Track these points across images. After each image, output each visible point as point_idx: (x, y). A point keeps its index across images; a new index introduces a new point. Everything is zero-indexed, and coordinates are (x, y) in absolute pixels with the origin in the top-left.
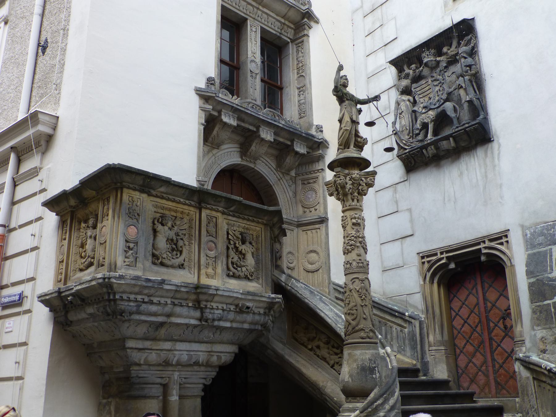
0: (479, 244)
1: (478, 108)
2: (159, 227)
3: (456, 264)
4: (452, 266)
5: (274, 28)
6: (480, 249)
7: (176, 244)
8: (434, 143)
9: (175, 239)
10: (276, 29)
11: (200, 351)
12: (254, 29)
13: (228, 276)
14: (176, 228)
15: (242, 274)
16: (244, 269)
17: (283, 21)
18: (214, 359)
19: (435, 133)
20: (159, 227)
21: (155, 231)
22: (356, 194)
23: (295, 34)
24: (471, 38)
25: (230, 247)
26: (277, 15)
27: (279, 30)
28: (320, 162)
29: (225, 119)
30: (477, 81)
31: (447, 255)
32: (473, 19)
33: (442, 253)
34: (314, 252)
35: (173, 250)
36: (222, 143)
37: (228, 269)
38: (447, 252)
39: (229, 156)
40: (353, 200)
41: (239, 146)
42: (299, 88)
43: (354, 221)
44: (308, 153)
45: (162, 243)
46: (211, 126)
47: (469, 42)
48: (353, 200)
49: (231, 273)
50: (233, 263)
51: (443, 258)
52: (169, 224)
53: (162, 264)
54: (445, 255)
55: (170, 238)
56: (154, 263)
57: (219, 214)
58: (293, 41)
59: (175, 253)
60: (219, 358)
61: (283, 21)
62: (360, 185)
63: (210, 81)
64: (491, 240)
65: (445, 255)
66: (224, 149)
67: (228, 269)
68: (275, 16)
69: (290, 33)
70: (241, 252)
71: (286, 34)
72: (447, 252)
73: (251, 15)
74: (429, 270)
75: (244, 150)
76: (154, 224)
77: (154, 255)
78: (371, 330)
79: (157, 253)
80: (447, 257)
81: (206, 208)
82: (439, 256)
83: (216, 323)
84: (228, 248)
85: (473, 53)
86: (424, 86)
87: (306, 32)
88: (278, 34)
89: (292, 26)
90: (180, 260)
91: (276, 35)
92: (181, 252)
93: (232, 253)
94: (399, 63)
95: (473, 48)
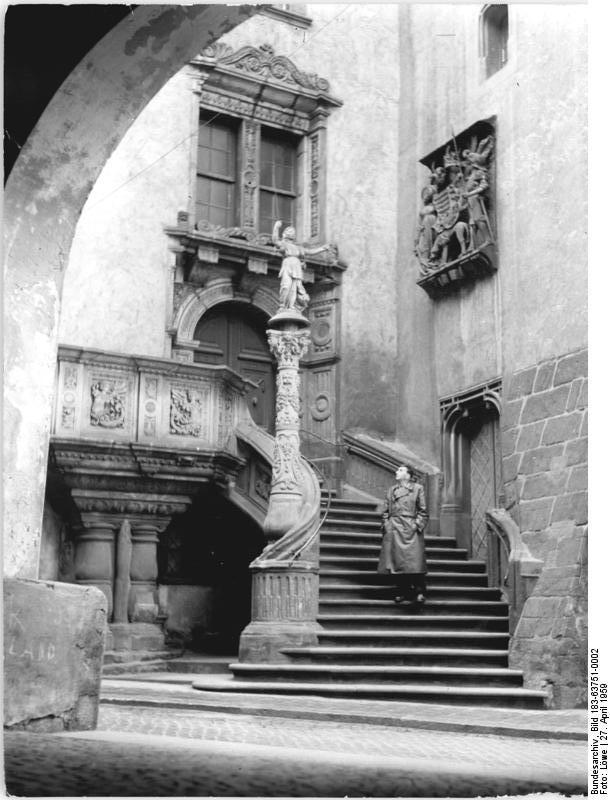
0: (481, 390)
1: (488, 229)
2: (96, 392)
3: (469, 411)
4: (466, 414)
5: (276, 121)
6: (482, 397)
7: (114, 407)
8: (446, 271)
9: (113, 403)
10: (284, 123)
11: (150, 500)
12: (251, 131)
13: (171, 433)
14: (114, 393)
15: (186, 432)
16: (188, 426)
17: (291, 111)
18: (164, 508)
20: (96, 392)
21: (93, 398)
22: (289, 354)
23: (311, 125)
24: (488, 142)
25: (174, 406)
26: (284, 107)
27: (288, 124)
28: (335, 290)
29: (203, 256)
30: (488, 199)
31: (462, 401)
32: (494, 118)
33: (456, 399)
34: (322, 397)
35: (111, 412)
36: (207, 280)
37: (171, 427)
39: (218, 291)
40: (286, 359)
41: (228, 280)
42: (312, 197)
43: (285, 381)
44: (316, 280)
46: (189, 264)
47: (485, 146)
48: (286, 359)
49: (174, 431)
50: (176, 421)
51: (455, 406)
53: (100, 425)
54: (458, 402)
55: (108, 401)
56: (92, 424)
57: (161, 377)
58: (308, 134)
59: (113, 415)
60: (169, 507)
61: (291, 111)
62: (292, 345)
63: (183, 217)
64: (491, 387)
65: (458, 402)
66: (212, 286)
67: (171, 427)
68: (280, 109)
70: (186, 410)
71: (298, 127)
73: (247, 113)
74: (446, 418)
75: (236, 286)
76: (92, 390)
77: (92, 418)
78: (292, 482)
79: (94, 416)
80: (460, 404)
81: (145, 372)
82: (453, 403)
83: (155, 476)
84: (171, 408)
85: (488, 162)
87: (320, 124)
88: (286, 129)
89: (305, 115)
90: (119, 421)
91: (283, 131)
92: (120, 413)
93: (175, 411)
94: (433, 160)
95: (490, 154)
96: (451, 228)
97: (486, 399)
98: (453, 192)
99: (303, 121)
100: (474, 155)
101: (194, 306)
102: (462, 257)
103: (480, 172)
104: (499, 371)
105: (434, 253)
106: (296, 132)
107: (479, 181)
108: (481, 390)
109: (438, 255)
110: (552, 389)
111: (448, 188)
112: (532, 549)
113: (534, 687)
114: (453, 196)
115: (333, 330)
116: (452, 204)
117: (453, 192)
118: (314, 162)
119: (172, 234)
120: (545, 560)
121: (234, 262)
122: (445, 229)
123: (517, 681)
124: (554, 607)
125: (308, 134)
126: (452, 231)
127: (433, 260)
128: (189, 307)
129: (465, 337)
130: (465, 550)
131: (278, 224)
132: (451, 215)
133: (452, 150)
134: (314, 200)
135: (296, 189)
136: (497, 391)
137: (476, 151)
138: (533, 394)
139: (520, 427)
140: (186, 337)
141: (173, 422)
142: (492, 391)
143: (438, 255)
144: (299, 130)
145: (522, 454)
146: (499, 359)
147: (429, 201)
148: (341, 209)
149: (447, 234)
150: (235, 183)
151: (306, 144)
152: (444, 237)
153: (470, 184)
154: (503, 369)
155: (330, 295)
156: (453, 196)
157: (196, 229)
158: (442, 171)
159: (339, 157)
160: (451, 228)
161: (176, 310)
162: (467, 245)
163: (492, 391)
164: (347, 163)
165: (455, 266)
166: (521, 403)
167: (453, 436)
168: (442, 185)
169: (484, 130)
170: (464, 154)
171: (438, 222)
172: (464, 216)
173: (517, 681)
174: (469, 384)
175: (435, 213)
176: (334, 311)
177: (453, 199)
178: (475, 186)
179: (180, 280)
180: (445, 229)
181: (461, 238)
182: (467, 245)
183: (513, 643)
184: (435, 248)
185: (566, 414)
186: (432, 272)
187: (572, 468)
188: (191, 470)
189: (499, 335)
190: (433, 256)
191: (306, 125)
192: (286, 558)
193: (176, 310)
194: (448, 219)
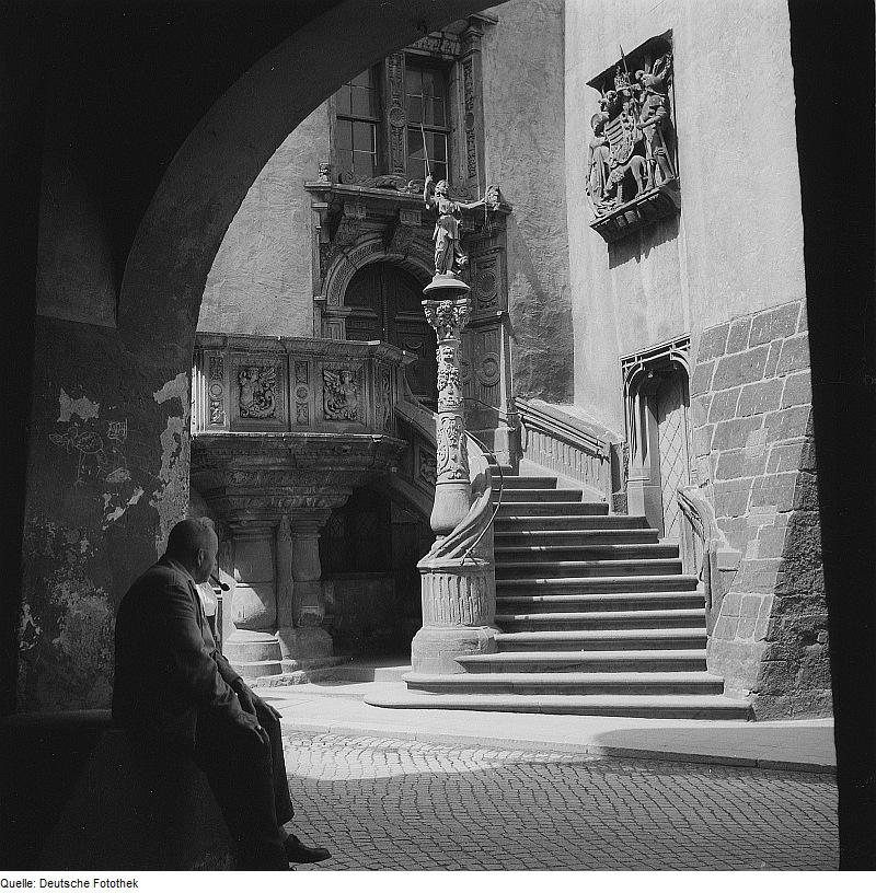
0: (667, 349)
8: (622, 212)
12: (395, 62)
19: (625, 199)
21: (242, 387)
32: (670, 33)
35: (261, 401)
37: (326, 413)
38: (644, 357)
39: (367, 251)
43: (446, 356)
45: (248, 399)
50: (330, 406)
52: (255, 377)
64: (678, 345)
69: (456, 48)
72: (644, 357)
74: (628, 380)
82: (636, 362)
85: (664, 86)
86: (615, 128)
93: (328, 395)
94: (603, 82)
95: (667, 76)
96: (627, 162)
97: (675, 358)
98: (627, 121)
99: (452, 44)
100: (648, 77)
101: (342, 271)
102: (638, 198)
103: (658, 98)
104: (687, 328)
105: (608, 191)
106: (447, 57)
107: (655, 108)
108: (667, 349)
109: (613, 194)
110: (748, 350)
111: (621, 116)
112: (730, 537)
113: (735, 696)
114: (627, 125)
115: (498, 284)
116: (627, 134)
117: (627, 121)
118: (468, 91)
119: (317, 192)
120: (744, 551)
121: (389, 218)
122: (619, 164)
123: (717, 688)
124: (757, 605)
125: (458, 58)
126: (627, 166)
127: (608, 199)
128: (337, 270)
129: (647, 287)
130: (656, 530)
131: (428, 179)
132: (626, 147)
133: (622, 71)
134: (470, 136)
135: (450, 123)
136: (685, 350)
137: (651, 73)
138: (726, 355)
139: (712, 393)
140: (336, 306)
141: (327, 409)
142: (679, 350)
143: (613, 194)
144: (450, 54)
145: (716, 425)
146: (687, 312)
147: (598, 134)
148: (501, 144)
149: (623, 169)
150: (379, 123)
151: (459, 71)
152: (617, 174)
153: (646, 110)
154: (692, 326)
155: (492, 245)
156: (627, 125)
157: (341, 183)
158: (614, 96)
159: (496, 83)
160: (627, 162)
161: (323, 274)
162: (645, 183)
163: (679, 350)
164: (505, 90)
165: (633, 207)
166: (712, 365)
167: (637, 398)
168: (615, 110)
169: (658, 49)
170: (637, 76)
171: (612, 155)
172: (640, 149)
173: (717, 688)
174: (653, 342)
175: (607, 144)
176: (498, 262)
177: (627, 129)
178: (650, 114)
179: (326, 240)
180: (619, 164)
181: (637, 176)
182: (645, 183)
183: (713, 641)
184: (608, 186)
185: (764, 380)
186: (607, 213)
187: (772, 444)
188: (348, 460)
189: (684, 285)
190: (606, 195)
191: (456, 48)
192: (458, 556)
193: (323, 274)
194: (623, 152)
